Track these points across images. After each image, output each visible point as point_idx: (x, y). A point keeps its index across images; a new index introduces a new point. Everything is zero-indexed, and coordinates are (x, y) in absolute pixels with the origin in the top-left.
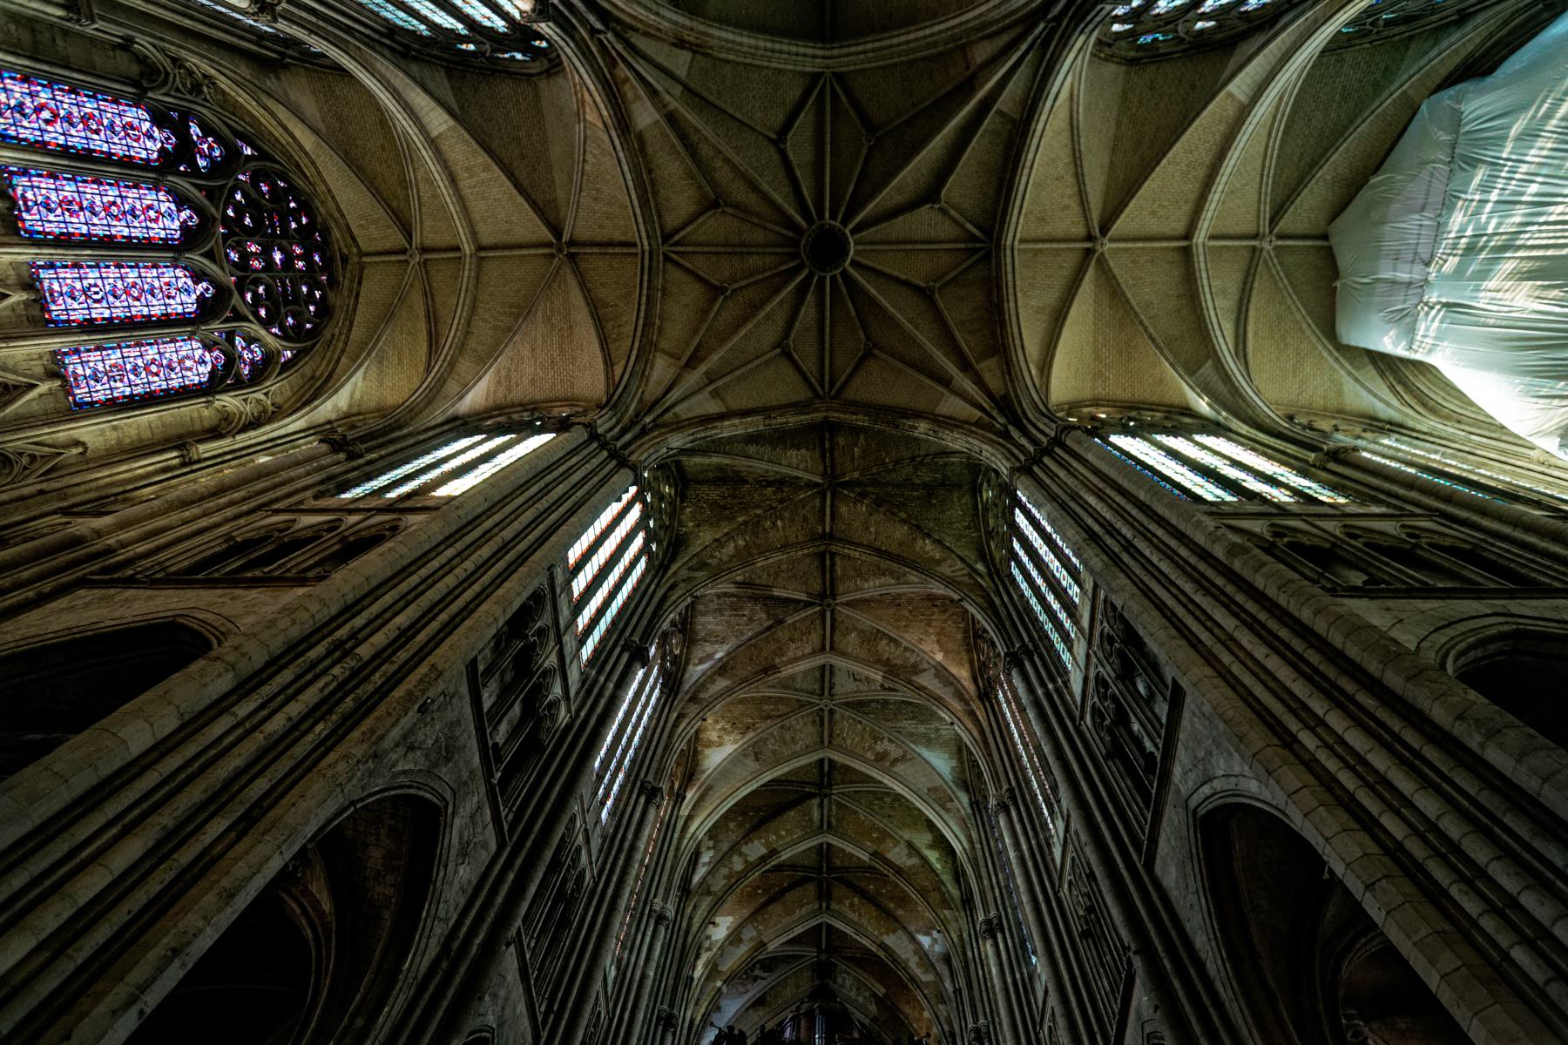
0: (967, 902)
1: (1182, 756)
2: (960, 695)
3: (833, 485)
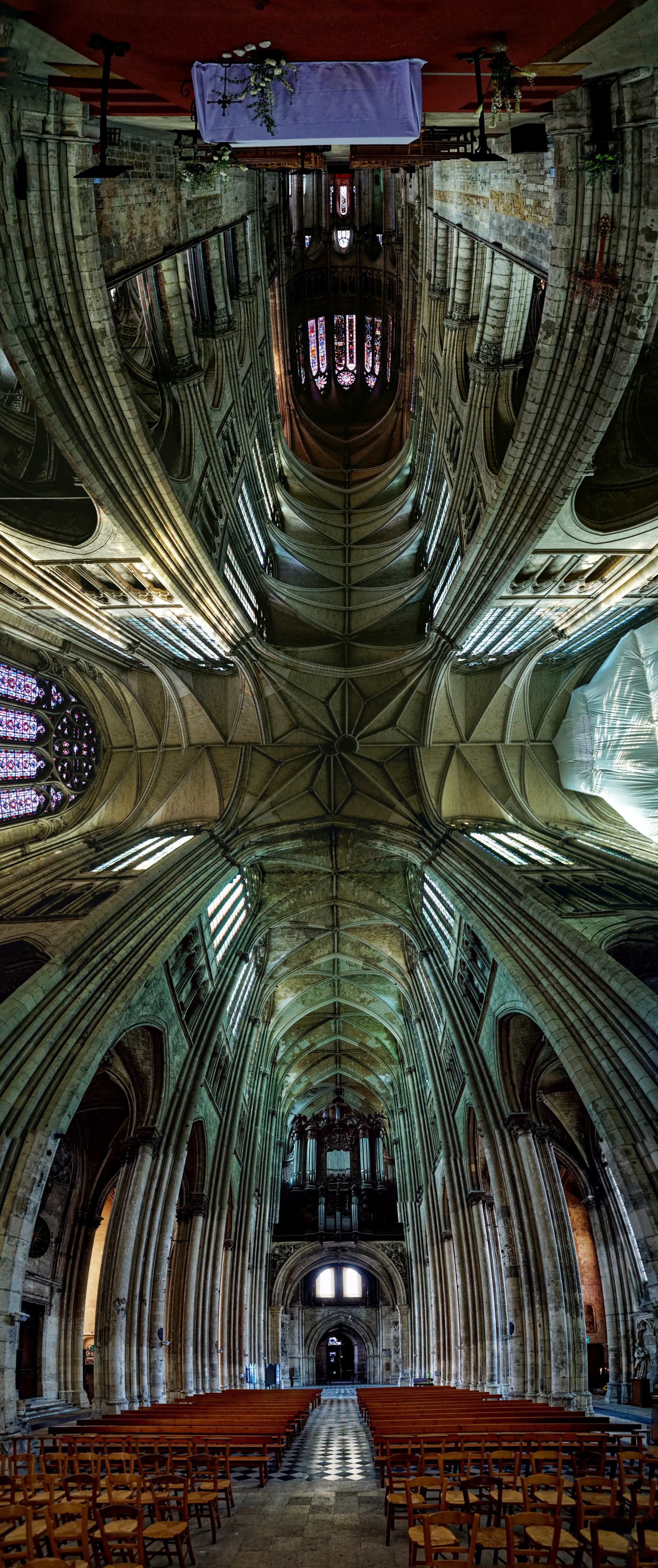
0: (401, 1061)
1: (494, 994)
2: (400, 972)
3: (337, 873)
